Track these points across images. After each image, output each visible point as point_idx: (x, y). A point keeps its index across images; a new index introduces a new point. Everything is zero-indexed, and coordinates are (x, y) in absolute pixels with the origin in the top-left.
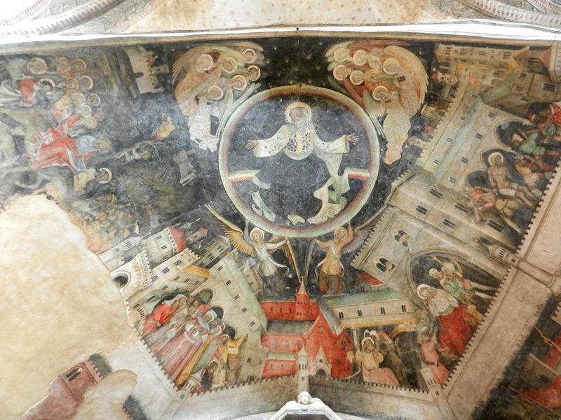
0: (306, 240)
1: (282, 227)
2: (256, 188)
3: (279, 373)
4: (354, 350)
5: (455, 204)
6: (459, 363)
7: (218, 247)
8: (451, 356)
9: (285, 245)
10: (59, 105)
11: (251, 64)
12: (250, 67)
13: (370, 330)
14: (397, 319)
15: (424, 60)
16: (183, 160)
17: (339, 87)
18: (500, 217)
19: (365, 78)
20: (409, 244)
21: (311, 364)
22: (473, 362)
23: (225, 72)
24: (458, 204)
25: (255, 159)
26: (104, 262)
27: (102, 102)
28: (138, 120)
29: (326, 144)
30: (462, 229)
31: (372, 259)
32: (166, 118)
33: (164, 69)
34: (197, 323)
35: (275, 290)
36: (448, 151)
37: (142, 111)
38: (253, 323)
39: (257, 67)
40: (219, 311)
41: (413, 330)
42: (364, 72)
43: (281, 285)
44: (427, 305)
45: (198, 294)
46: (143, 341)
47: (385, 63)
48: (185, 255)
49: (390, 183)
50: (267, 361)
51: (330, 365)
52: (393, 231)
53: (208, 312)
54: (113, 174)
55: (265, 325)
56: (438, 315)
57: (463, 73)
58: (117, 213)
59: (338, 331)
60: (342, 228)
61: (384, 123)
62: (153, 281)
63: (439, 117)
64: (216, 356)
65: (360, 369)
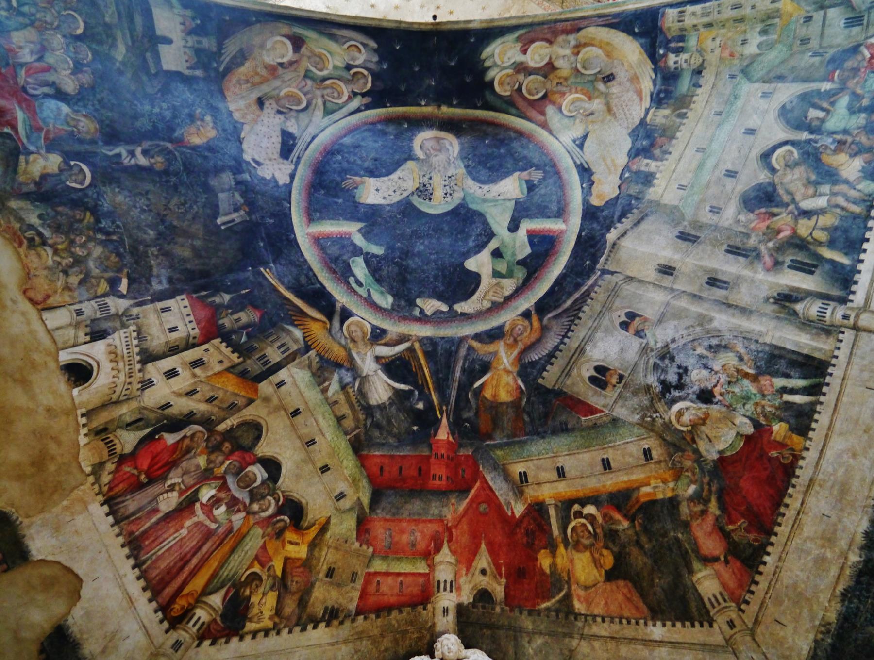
0: (450, 340)
1: (405, 318)
2: (357, 251)
3: (393, 600)
4: (552, 548)
5: (725, 247)
6: (769, 549)
7: (279, 344)
8: (752, 536)
9: (411, 350)
11: (357, 66)
13: (583, 505)
14: (637, 476)
15: (643, 41)
16: (227, 187)
17: (504, 106)
18: (808, 250)
19: (549, 86)
20: (647, 332)
21: (462, 580)
22: (797, 541)
23: (310, 71)
24: (729, 246)
25: (356, 205)
26: (49, 326)
27: (94, 59)
28: (153, 106)
29: (486, 187)
30: (744, 289)
31: (579, 369)
32: (204, 116)
34: (224, 487)
35: (390, 433)
36: (701, 166)
37: (162, 95)
38: (341, 496)
39: (365, 72)
40: (273, 466)
41: (669, 494)
42: (545, 77)
43: (401, 422)
44: (694, 441)
45: (232, 428)
46: (106, 508)
47: (580, 56)
48: (212, 350)
49: (603, 236)
50: (369, 574)
51: (504, 581)
52: (615, 315)
53: (249, 468)
54: (93, 178)
55: (366, 501)
56: (715, 456)
57: (709, 44)
58: (91, 245)
59: (519, 509)
60: (519, 318)
61: (586, 144)
62: (143, 389)
63: (678, 120)
64: (262, 558)
65: (566, 586)
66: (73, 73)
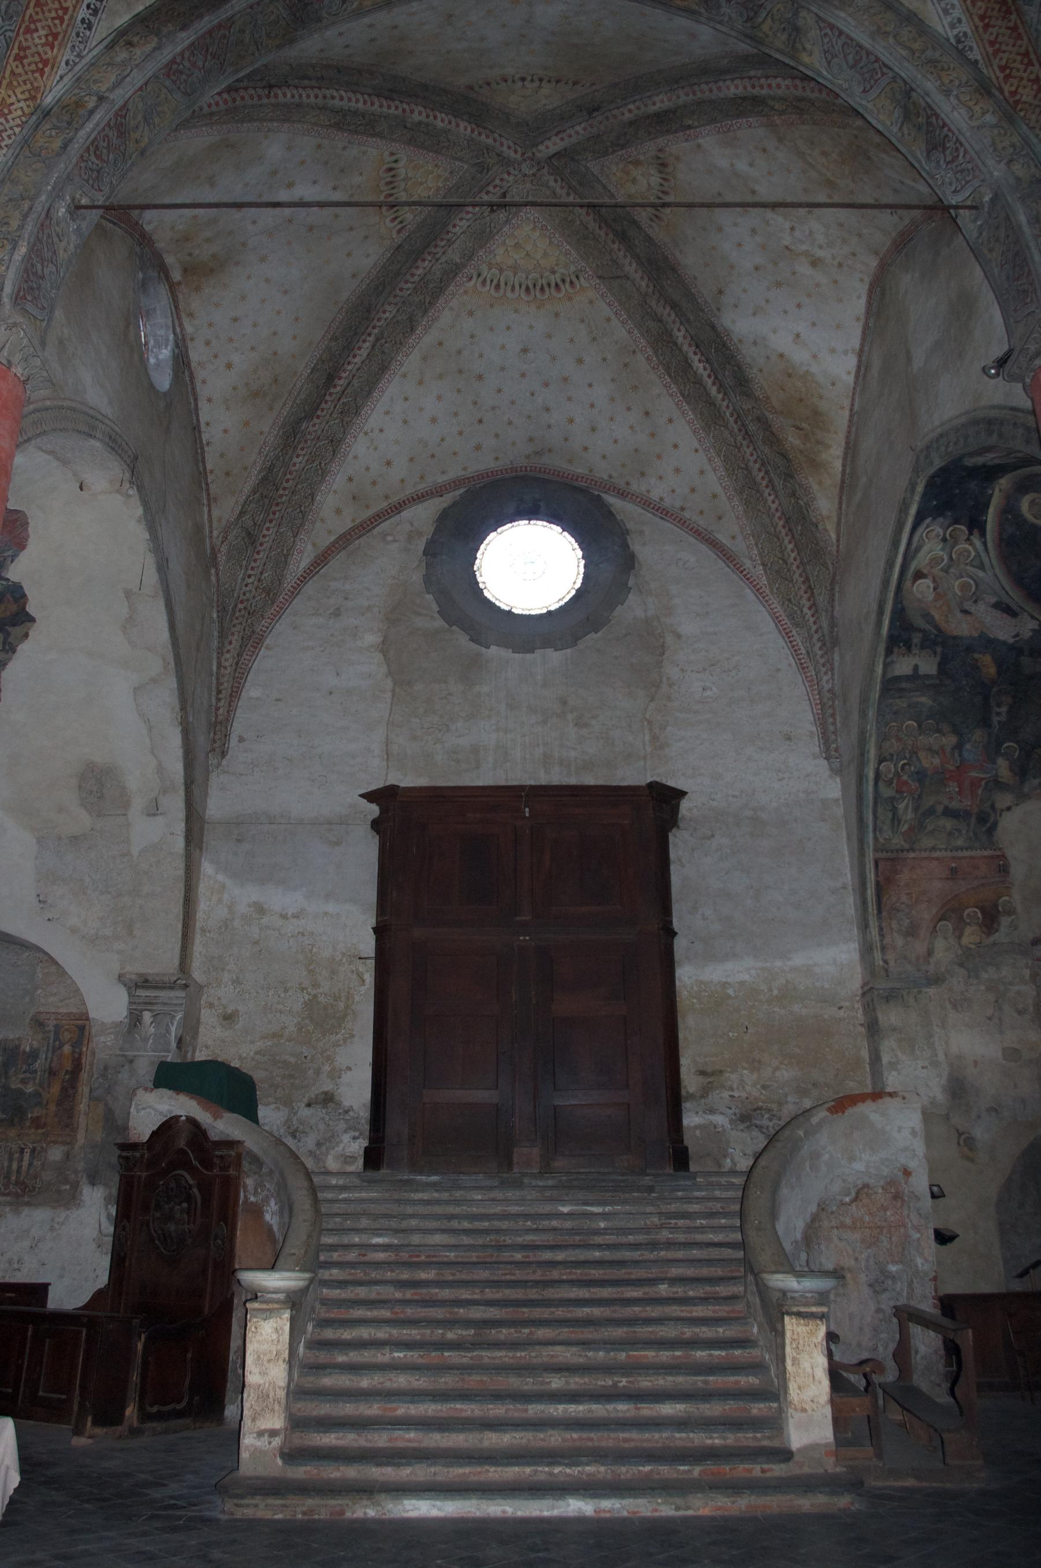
10: (926, 764)
11: (945, 534)
12: (948, 536)
33: (917, 638)
39: (951, 528)
66: (944, 735)
